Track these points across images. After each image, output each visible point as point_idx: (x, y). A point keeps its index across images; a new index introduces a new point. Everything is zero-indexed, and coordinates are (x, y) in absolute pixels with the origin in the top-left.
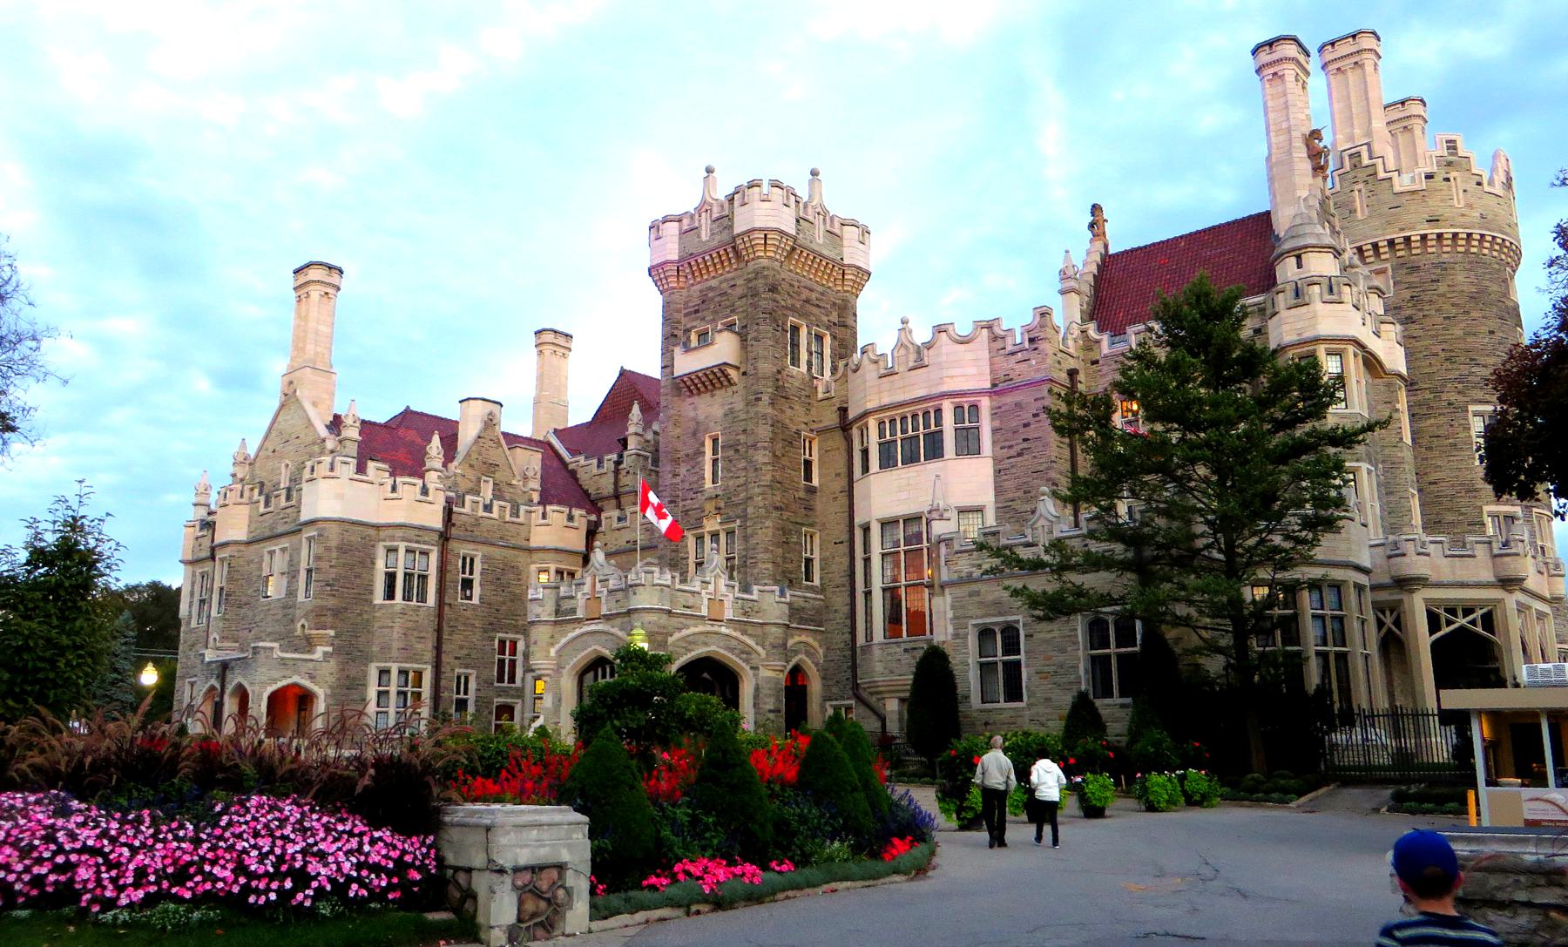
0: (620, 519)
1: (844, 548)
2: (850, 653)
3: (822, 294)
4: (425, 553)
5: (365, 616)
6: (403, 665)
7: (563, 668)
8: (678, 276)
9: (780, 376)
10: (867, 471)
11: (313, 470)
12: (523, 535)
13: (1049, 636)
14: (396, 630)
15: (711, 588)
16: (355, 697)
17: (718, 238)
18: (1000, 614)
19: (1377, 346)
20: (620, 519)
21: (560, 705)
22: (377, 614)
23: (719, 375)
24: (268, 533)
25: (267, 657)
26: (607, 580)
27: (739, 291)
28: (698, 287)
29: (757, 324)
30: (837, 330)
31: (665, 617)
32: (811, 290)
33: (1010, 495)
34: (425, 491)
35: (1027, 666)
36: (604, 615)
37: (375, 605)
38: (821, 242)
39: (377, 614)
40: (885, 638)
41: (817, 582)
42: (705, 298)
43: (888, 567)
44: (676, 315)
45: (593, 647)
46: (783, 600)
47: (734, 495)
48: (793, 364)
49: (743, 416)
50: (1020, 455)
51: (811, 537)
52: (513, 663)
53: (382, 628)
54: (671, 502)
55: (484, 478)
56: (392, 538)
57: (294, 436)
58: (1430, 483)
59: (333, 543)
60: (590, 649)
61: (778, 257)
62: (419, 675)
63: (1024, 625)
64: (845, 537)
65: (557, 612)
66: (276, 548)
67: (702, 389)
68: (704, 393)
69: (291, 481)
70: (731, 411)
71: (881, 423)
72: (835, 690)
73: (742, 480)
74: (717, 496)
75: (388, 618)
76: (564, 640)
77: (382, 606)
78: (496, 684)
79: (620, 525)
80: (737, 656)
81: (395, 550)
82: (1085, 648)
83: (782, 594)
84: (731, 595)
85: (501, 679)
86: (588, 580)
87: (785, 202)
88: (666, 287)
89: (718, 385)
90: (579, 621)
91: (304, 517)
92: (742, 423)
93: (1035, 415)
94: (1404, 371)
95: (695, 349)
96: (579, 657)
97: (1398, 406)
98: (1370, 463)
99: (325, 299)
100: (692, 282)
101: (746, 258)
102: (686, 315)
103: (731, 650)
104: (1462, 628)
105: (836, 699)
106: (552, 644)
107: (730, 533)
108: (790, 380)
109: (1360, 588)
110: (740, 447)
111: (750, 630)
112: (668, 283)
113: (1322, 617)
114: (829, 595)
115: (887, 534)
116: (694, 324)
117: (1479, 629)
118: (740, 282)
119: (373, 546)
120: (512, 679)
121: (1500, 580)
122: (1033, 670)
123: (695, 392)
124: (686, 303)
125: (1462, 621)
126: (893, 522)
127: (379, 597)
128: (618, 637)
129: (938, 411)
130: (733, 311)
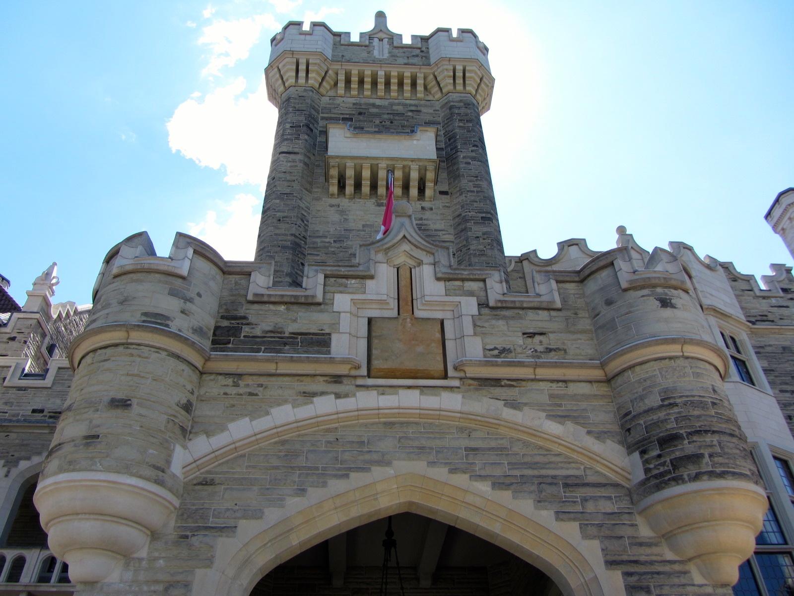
7: (229, 530)
17: (401, 61)
28: (353, 100)
49: (450, 238)
67: (366, 189)
102: (323, 118)
106: (185, 433)
118: (424, 110)
123: (349, 189)
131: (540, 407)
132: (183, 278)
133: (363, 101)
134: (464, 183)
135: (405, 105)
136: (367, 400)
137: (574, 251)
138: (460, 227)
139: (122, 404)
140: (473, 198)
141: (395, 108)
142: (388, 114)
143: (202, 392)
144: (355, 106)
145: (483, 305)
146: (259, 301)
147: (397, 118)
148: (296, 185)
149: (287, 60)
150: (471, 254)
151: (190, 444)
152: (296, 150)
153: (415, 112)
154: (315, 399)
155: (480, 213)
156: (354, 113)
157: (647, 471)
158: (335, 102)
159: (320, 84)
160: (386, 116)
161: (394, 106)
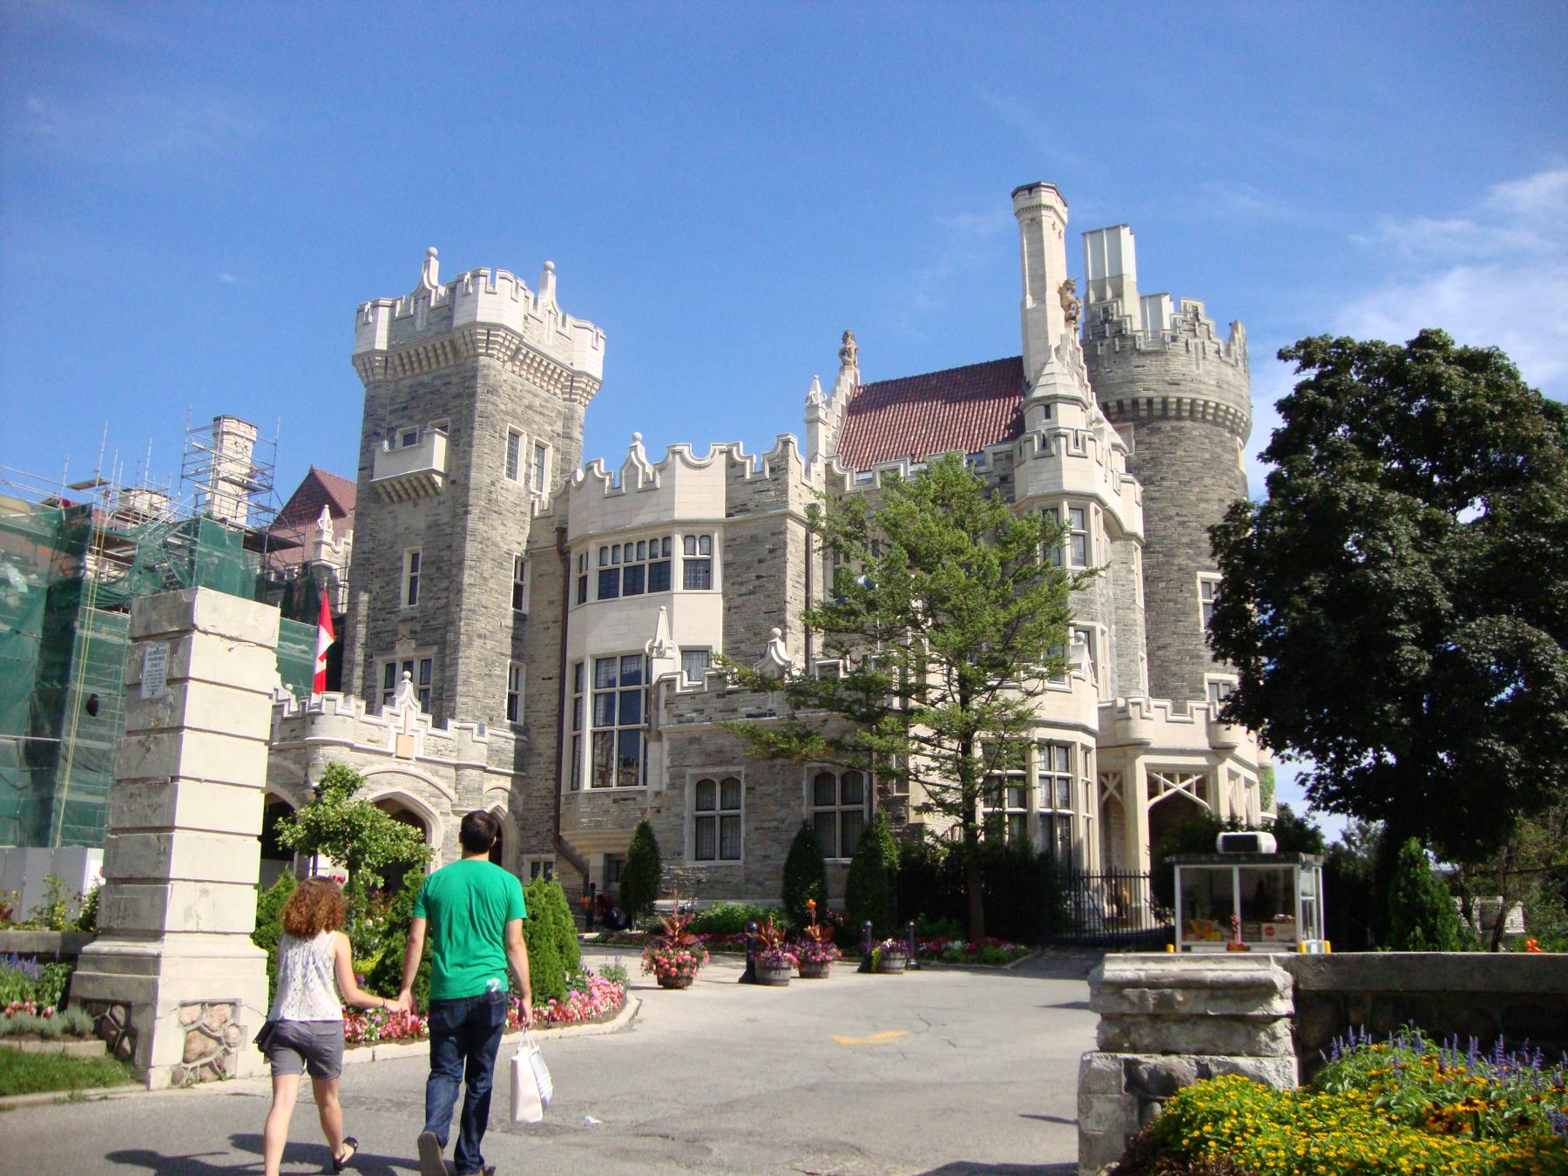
1: (554, 685)
2: (553, 801)
3: (546, 401)
8: (386, 367)
9: (493, 488)
10: (585, 600)
13: (772, 789)
15: (400, 722)
17: (434, 329)
18: (721, 763)
19: (1114, 503)
23: (425, 482)
27: (454, 390)
28: (408, 382)
30: (559, 442)
31: (347, 750)
32: (536, 396)
33: (739, 637)
35: (747, 821)
38: (550, 344)
40: (593, 786)
41: (520, 721)
43: (601, 706)
46: (481, 739)
48: (509, 476)
49: (448, 530)
50: (751, 593)
51: (517, 670)
58: (1159, 648)
61: (501, 355)
63: (746, 776)
64: (555, 672)
70: (436, 524)
71: (603, 549)
72: (533, 842)
74: (413, 618)
80: (426, 799)
82: (809, 804)
83: (481, 732)
84: (423, 733)
87: (514, 296)
88: (371, 379)
89: (422, 493)
93: (771, 551)
94: (1141, 534)
97: (1133, 567)
98: (1104, 622)
100: (401, 375)
101: (465, 354)
102: (391, 412)
103: (421, 792)
104: (1177, 795)
105: (535, 852)
107: (426, 662)
108: (504, 492)
109: (1086, 750)
111: (443, 770)
112: (374, 375)
113: (1049, 778)
114: (533, 736)
115: (602, 670)
117: (1193, 795)
118: (455, 380)
121: (1214, 748)
122: (752, 826)
123: (395, 498)
124: (393, 399)
125: (1179, 787)
126: (610, 659)
129: (667, 539)
130: (446, 412)
159: (386, 373)
160: (429, 397)
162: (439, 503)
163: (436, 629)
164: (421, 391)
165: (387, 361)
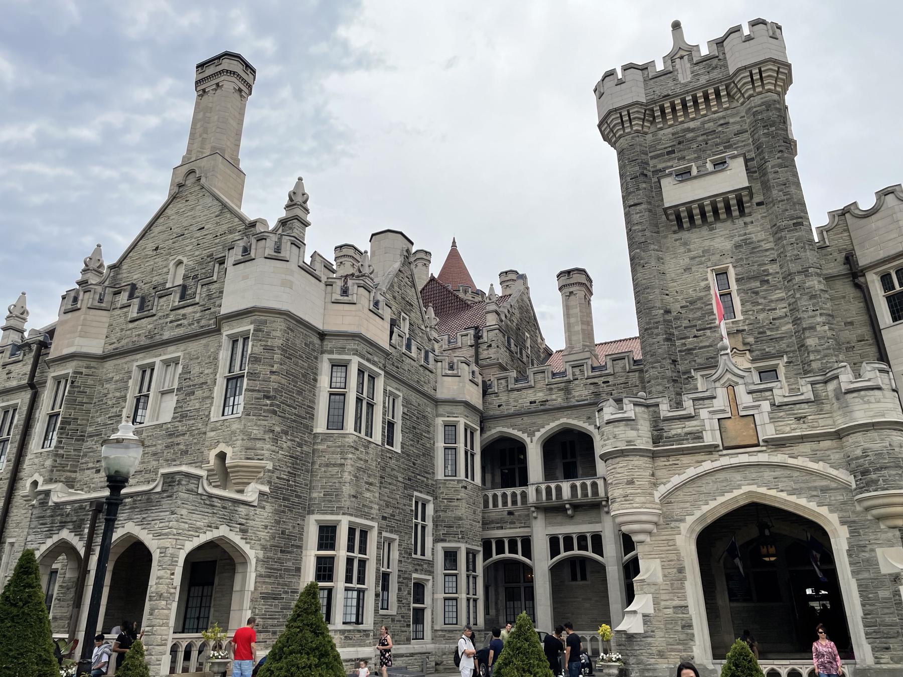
0: (517, 380)
4: (372, 378)
5: (305, 448)
6: (353, 519)
7: (682, 520)
11: (246, 250)
12: (432, 383)
14: (348, 468)
16: (290, 564)
17: (703, 80)
20: (517, 380)
21: (683, 580)
22: (320, 447)
23: (733, 202)
24: (144, 341)
25: (189, 491)
26: (771, 390)
27: (737, 128)
29: (781, 151)
34: (376, 304)
36: (764, 441)
37: (316, 436)
39: (320, 447)
42: (681, 139)
44: (644, 157)
45: (745, 489)
47: (771, 329)
49: (768, 246)
52: (423, 528)
53: (327, 465)
54: (667, 340)
55: (403, 314)
56: (342, 350)
57: (194, 228)
59: (278, 342)
60: (736, 493)
62: (364, 534)
65: (656, 441)
66: (157, 360)
67: (698, 221)
68: (700, 227)
69: (186, 277)
73: (779, 313)
75: (333, 453)
76: (676, 480)
77: (326, 437)
78: (414, 556)
79: (518, 386)
81: (345, 365)
85: (416, 553)
86: (721, 393)
89: (723, 216)
90: (711, 450)
91: (228, 306)
92: (768, 253)
95: (695, 177)
96: (713, 504)
99: (237, 95)
100: (660, 126)
102: (652, 158)
106: (655, 485)
110: (766, 278)
112: (631, 126)
116: (669, 164)
119: (316, 358)
120: (423, 554)
127: (320, 427)
128: (811, 473)
130: (729, 147)
131: (806, 456)
132: (633, 420)
133: (680, 127)
134: (775, 192)
135: (714, 120)
136: (725, 461)
137: (890, 197)
138: (779, 235)
139: (631, 482)
140: (784, 207)
141: (706, 126)
142: (702, 135)
143: (656, 465)
144: (674, 137)
145: (773, 405)
146: (667, 419)
147: (710, 137)
148: (648, 233)
149: (613, 117)
150: (788, 261)
151: (658, 489)
152: (640, 201)
153: (724, 126)
154: (703, 463)
155: (791, 220)
156: (674, 143)
157: (857, 485)
158: (657, 137)
159: (643, 126)
160: (700, 138)
161: (705, 125)
162: (745, 223)
163: (782, 338)
164: (690, 135)
165: (645, 113)
